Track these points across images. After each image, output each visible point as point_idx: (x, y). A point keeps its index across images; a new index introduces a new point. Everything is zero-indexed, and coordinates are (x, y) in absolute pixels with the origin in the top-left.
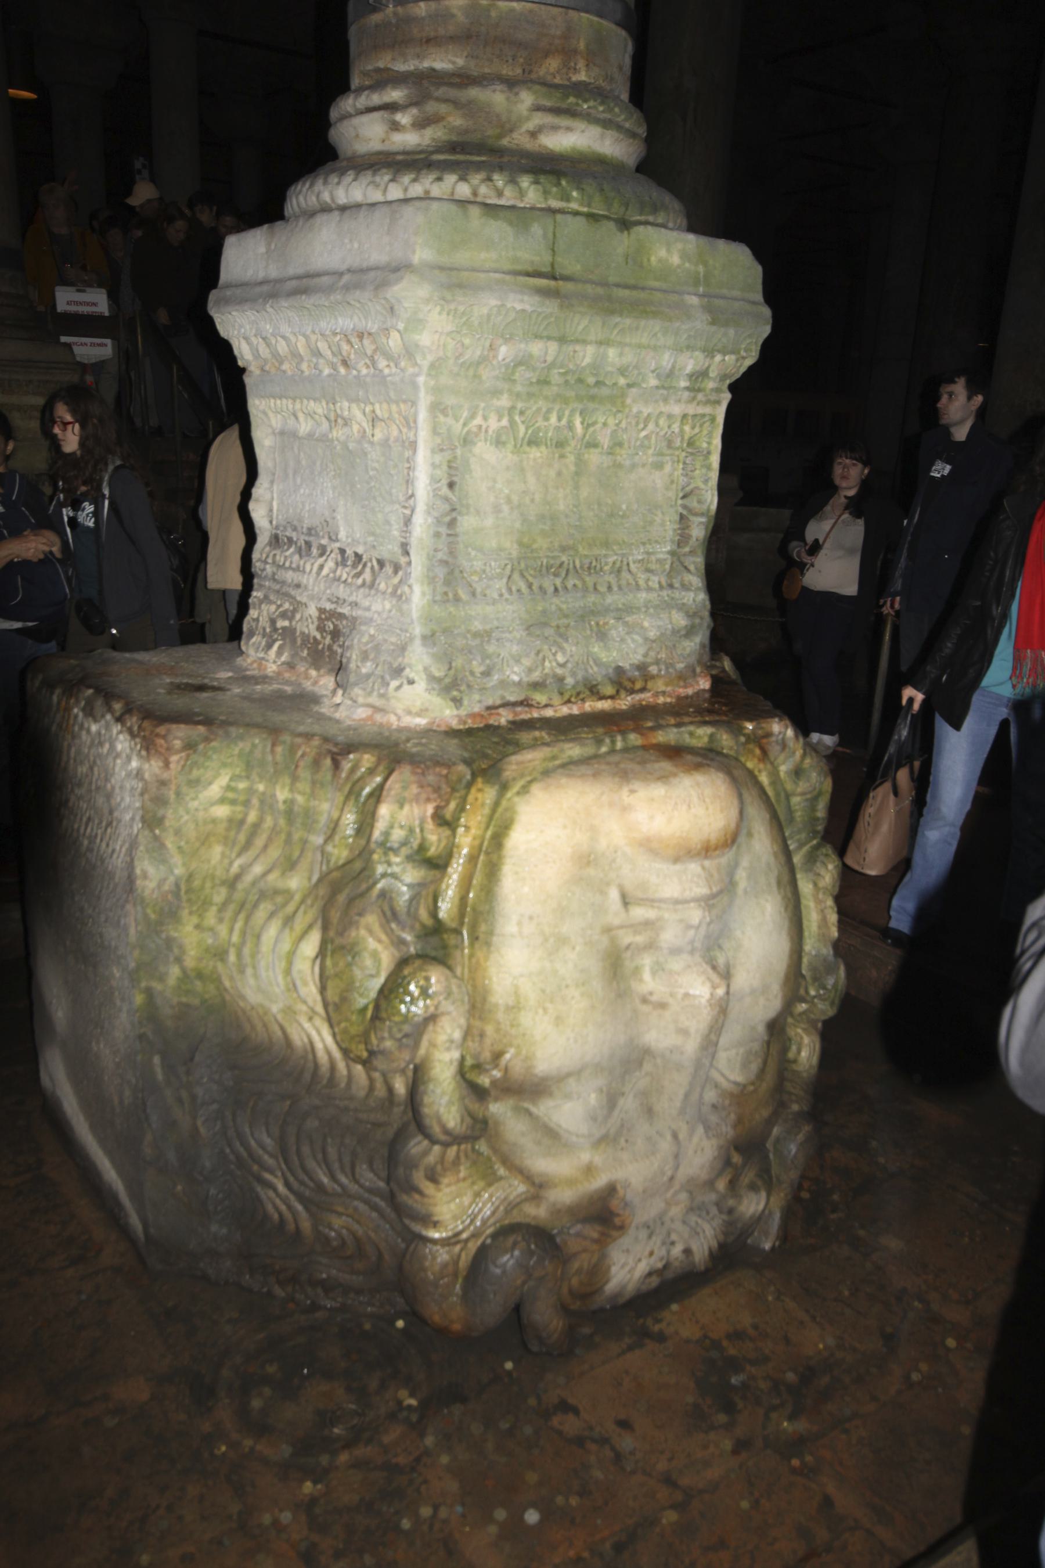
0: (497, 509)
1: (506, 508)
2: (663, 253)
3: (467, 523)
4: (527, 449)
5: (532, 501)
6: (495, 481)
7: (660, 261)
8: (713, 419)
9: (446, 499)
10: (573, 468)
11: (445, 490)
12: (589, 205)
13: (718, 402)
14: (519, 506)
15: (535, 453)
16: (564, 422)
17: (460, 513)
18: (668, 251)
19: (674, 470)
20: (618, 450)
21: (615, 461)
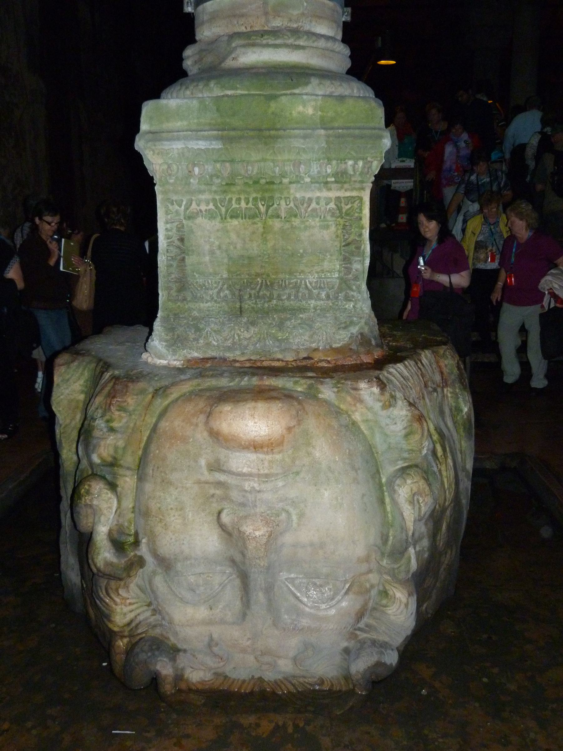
0: (212, 253)
1: (218, 252)
2: (301, 108)
3: (190, 260)
4: (229, 220)
5: (235, 248)
6: (210, 238)
7: (299, 113)
8: (361, 199)
9: (178, 247)
10: (261, 230)
11: (178, 243)
12: (248, 90)
13: (363, 189)
14: (226, 251)
15: (235, 222)
16: (250, 205)
17: (188, 255)
18: (304, 106)
19: (337, 229)
20: (293, 219)
21: (292, 225)
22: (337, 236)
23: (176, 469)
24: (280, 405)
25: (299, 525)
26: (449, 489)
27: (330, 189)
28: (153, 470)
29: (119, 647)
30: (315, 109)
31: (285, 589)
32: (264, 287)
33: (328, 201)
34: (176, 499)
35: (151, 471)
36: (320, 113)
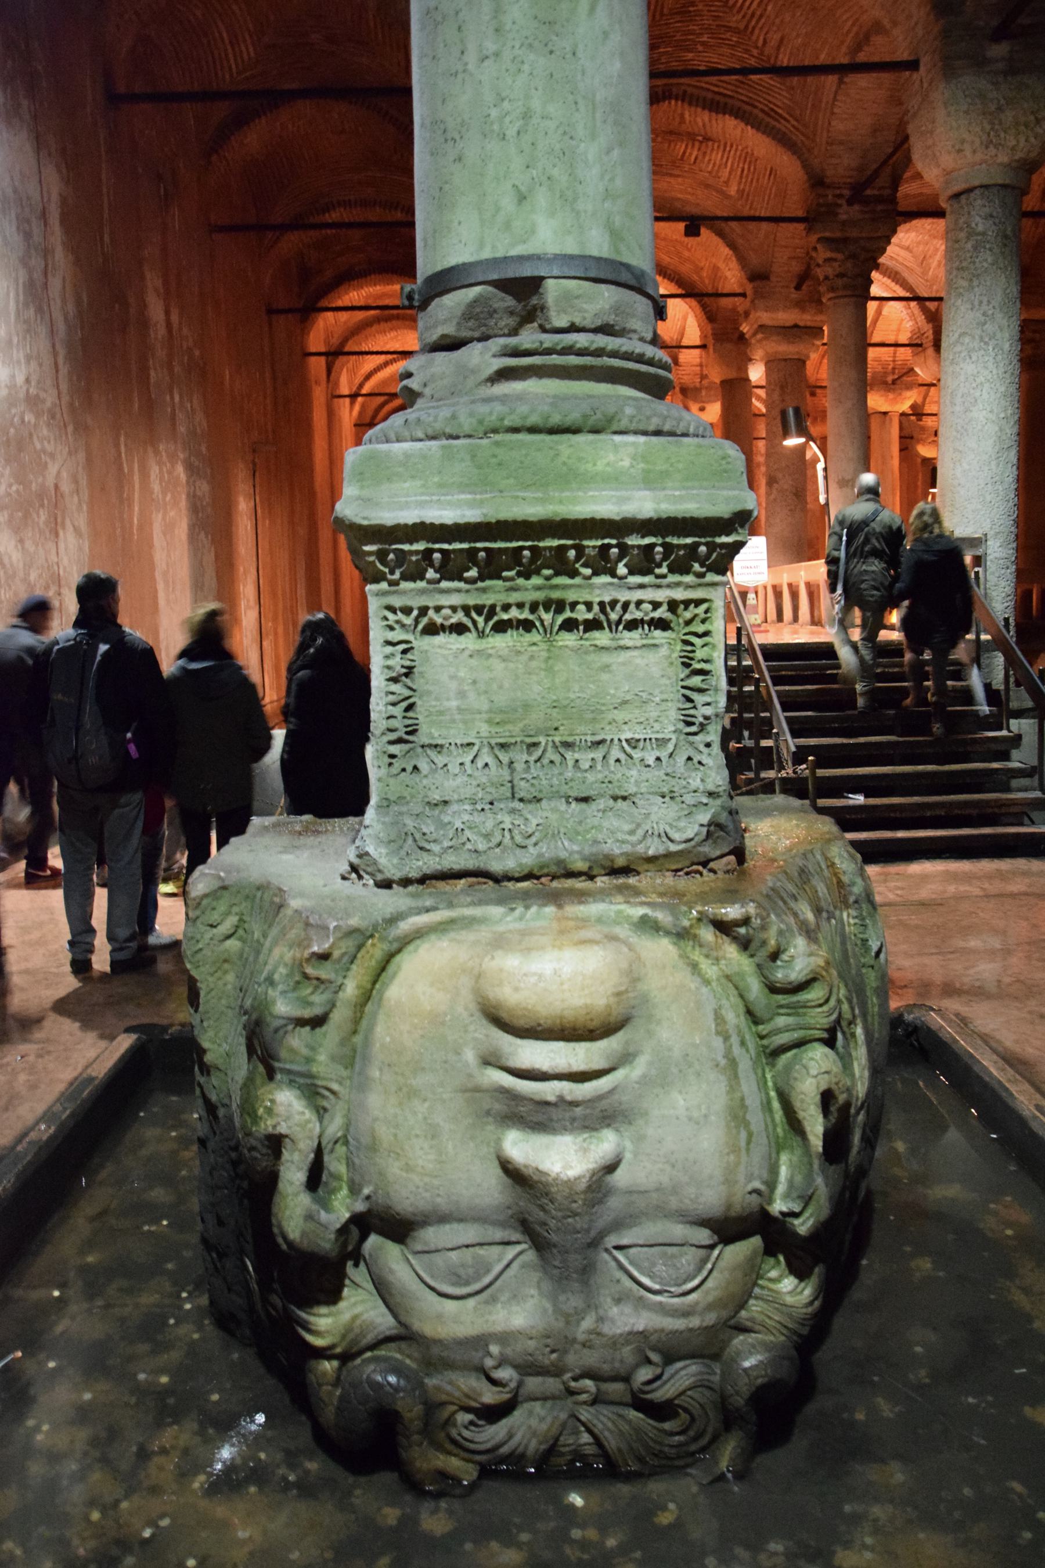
2: (611, 457)
5: (501, 687)
22: (672, 663)
23: (423, 1069)
24: (601, 953)
25: (636, 1155)
26: (861, 1077)
27: (659, 586)
28: (381, 1070)
29: (325, 1374)
30: (634, 458)
31: (613, 1264)
32: (549, 749)
33: (656, 605)
34: (425, 1118)
35: (378, 1074)
36: (642, 465)
